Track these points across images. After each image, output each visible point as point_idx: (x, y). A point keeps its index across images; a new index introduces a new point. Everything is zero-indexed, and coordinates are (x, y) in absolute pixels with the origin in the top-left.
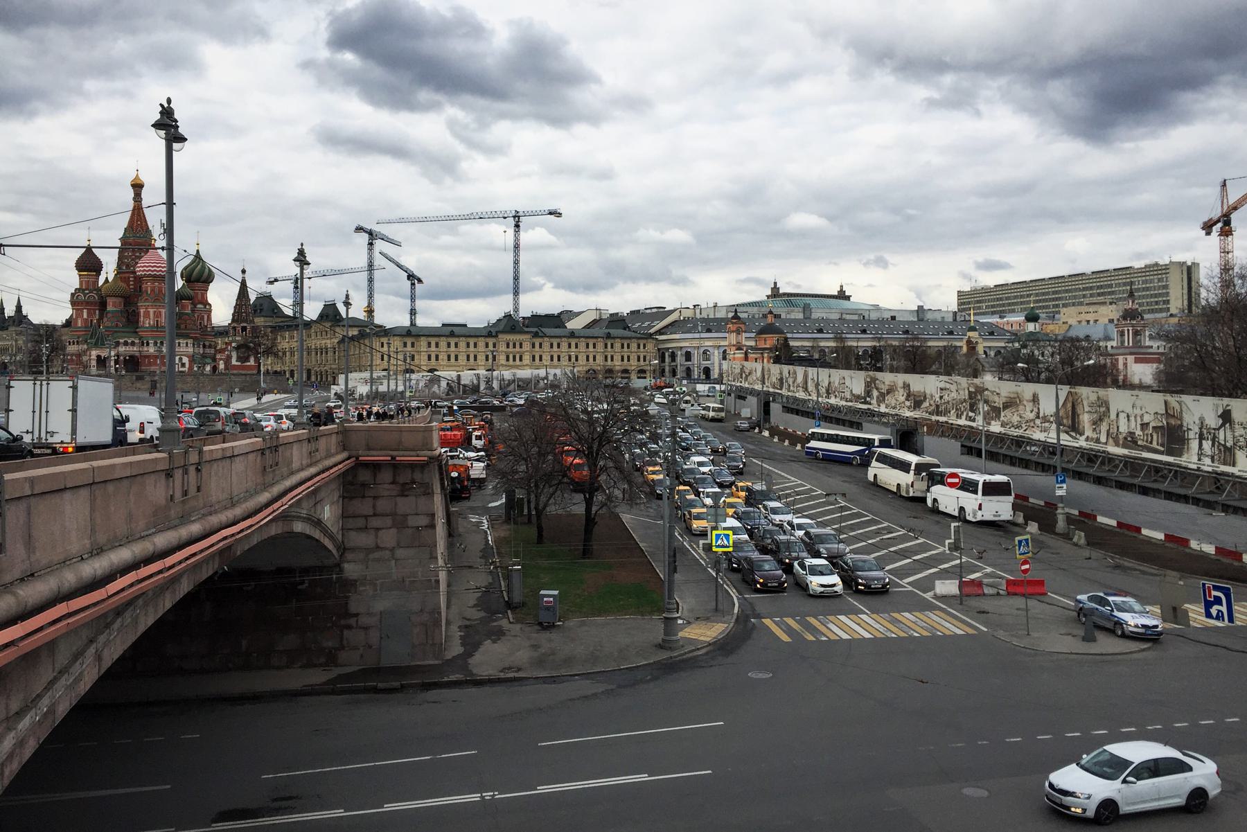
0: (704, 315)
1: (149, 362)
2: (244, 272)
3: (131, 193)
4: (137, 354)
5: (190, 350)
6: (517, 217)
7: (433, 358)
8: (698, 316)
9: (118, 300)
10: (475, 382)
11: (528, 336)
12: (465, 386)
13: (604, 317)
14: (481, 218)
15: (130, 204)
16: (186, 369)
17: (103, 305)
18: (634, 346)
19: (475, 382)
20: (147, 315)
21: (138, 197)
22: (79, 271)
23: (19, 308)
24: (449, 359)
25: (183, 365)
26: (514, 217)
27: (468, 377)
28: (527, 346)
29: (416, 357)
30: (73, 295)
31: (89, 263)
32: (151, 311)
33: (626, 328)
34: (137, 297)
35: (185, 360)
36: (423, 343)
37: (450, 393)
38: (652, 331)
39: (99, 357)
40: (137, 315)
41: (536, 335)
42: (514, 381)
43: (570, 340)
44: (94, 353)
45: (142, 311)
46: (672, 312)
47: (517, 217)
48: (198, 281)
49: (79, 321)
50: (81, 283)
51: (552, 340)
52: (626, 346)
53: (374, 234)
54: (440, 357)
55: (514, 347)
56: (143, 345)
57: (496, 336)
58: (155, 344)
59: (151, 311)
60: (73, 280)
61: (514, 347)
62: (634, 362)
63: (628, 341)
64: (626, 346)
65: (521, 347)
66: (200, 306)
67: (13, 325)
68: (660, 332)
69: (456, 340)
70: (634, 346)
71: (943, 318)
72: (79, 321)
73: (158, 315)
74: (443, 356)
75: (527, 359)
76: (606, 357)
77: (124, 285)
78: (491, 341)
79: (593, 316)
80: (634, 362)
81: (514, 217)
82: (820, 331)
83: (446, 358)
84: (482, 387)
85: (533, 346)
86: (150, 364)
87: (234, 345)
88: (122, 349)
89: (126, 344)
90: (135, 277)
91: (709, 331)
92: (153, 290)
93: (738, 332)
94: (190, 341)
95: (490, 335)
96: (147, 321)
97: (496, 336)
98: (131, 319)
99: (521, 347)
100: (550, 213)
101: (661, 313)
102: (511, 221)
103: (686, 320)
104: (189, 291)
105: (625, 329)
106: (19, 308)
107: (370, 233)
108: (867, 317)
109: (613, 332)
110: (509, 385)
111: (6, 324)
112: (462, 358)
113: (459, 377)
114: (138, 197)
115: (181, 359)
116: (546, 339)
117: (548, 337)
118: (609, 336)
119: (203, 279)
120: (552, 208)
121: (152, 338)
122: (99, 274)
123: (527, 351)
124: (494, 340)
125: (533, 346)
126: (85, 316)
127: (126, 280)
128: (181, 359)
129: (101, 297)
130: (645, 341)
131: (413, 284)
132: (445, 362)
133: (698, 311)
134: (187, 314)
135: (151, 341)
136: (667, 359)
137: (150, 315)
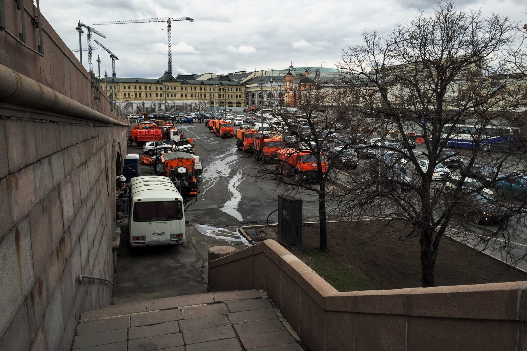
0: (267, 75)
6: (169, 21)
7: (127, 95)
8: (264, 75)
10: (153, 106)
11: (179, 84)
12: (147, 108)
13: (214, 77)
14: (149, 22)
18: (234, 89)
19: (153, 106)
26: (168, 21)
27: (148, 104)
28: (178, 89)
29: (117, 94)
33: (230, 80)
36: (121, 86)
37: (139, 112)
41: (183, 83)
42: (174, 106)
43: (201, 86)
47: (169, 21)
51: (192, 86)
52: (230, 89)
53: (91, 30)
54: (131, 94)
55: (172, 89)
57: (162, 83)
61: (172, 89)
62: (234, 98)
63: (232, 87)
64: (230, 89)
65: (175, 89)
69: (140, 85)
70: (234, 89)
74: (132, 94)
75: (179, 96)
76: (220, 95)
78: (159, 86)
79: (209, 77)
80: (234, 98)
81: (168, 21)
83: (134, 95)
84: (157, 109)
85: (182, 89)
97: (162, 83)
99: (175, 89)
100: (187, 19)
101: (244, 74)
102: (166, 24)
103: (258, 78)
105: (229, 81)
109: (224, 82)
110: (171, 108)
113: (143, 103)
116: (189, 85)
117: (189, 84)
118: (221, 84)
120: (188, 16)
123: (178, 92)
125: (182, 89)
130: (240, 87)
131: (113, 60)
132: (134, 97)
133: (264, 73)
136: (250, 98)
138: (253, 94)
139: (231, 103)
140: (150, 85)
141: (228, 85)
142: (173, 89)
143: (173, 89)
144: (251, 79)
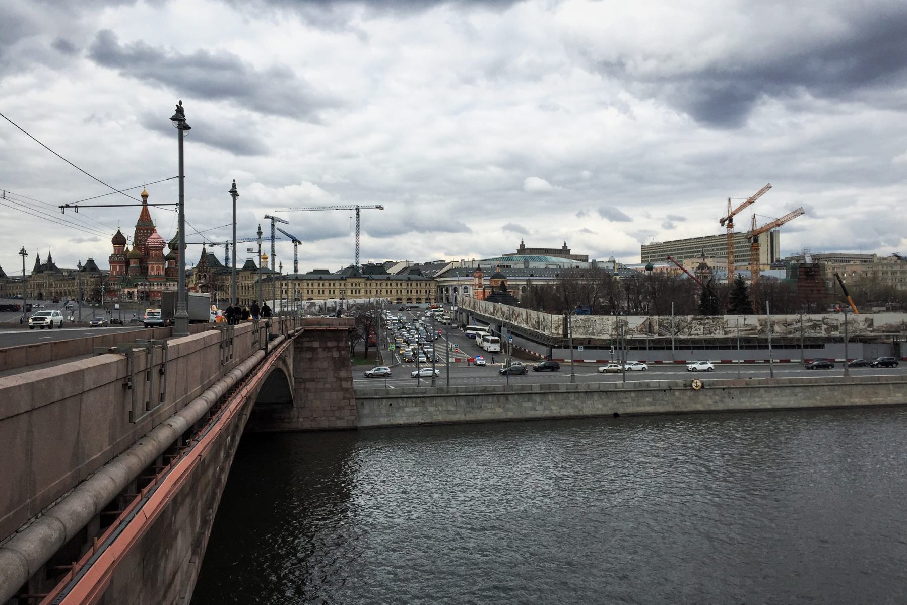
1: (154, 295)
6: (358, 209)
7: (310, 292)
8: (463, 267)
9: (136, 260)
10: (334, 305)
12: (328, 308)
13: (410, 266)
17: (127, 263)
18: (423, 284)
19: (334, 305)
20: (153, 269)
23: (50, 259)
24: (319, 292)
26: (356, 209)
27: (330, 303)
28: (363, 285)
30: (110, 258)
31: (119, 240)
33: (420, 274)
36: (305, 283)
38: (435, 276)
39: (129, 292)
40: (147, 268)
41: (368, 279)
42: (355, 305)
44: (126, 290)
45: (150, 266)
46: (449, 264)
47: (358, 209)
49: (115, 272)
50: (115, 251)
52: (419, 284)
54: (314, 292)
55: (356, 286)
56: (151, 285)
57: (346, 280)
58: (157, 285)
59: (155, 267)
60: (110, 249)
61: (356, 286)
63: (420, 282)
64: (419, 284)
65: (359, 286)
67: (47, 270)
68: (440, 276)
69: (323, 282)
70: (423, 284)
71: (607, 267)
72: (115, 272)
73: (158, 269)
74: (316, 291)
76: (408, 291)
77: (138, 252)
78: (343, 282)
79: (404, 265)
81: (356, 209)
82: (532, 275)
83: (317, 292)
87: (199, 285)
88: (139, 287)
89: (141, 285)
90: (144, 248)
91: (467, 276)
92: (156, 255)
93: (480, 277)
94: (176, 283)
95: (342, 279)
96: (152, 273)
97: (346, 280)
98: (143, 271)
99: (359, 286)
100: (377, 207)
101: (443, 264)
102: (354, 212)
103: (456, 269)
104: (174, 255)
105: (419, 275)
106: (50, 259)
107: (272, 218)
108: (562, 267)
109: (412, 277)
110: (352, 307)
112: (327, 293)
113: (325, 303)
116: (373, 281)
118: (409, 279)
120: (378, 204)
121: (156, 281)
122: (124, 246)
124: (344, 282)
126: (118, 269)
127: (140, 249)
129: (126, 258)
130: (430, 282)
131: (296, 245)
133: (463, 263)
134: (173, 268)
136: (445, 292)
137: (154, 269)
138: (447, 288)
139: (420, 299)
140: (334, 282)
141: (416, 280)
142: (358, 284)
143: (358, 284)
144: (447, 271)
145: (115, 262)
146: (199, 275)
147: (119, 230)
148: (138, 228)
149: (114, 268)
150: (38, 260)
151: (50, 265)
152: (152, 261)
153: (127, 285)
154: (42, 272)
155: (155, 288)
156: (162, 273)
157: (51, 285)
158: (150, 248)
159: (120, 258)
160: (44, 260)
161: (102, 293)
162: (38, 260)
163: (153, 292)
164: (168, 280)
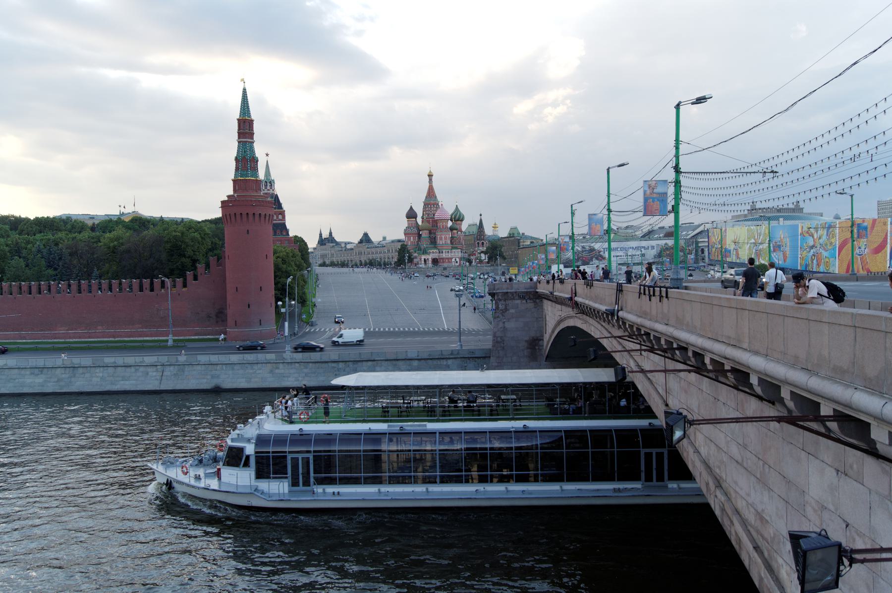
2: (481, 215)
3: (428, 178)
4: (438, 257)
5: (460, 255)
15: (428, 185)
16: (458, 264)
20: (441, 238)
21: (430, 180)
22: (407, 218)
23: (331, 234)
25: (457, 262)
30: (405, 230)
31: (411, 214)
32: (443, 237)
34: (436, 230)
35: (458, 260)
39: (425, 259)
44: (423, 257)
46: (699, 226)
48: (458, 220)
50: (409, 224)
60: (404, 223)
66: (459, 233)
77: (428, 224)
86: (443, 262)
89: (433, 252)
92: (443, 227)
98: (433, 242)
106: (331, 234)
111: (324, 242)
114: (430, 180)
115: (456, 260)
119: (461, 219)
127: (428, 222)
128: (456, 260)
135: (444, 251)
137: (444, 238)
145: (410, 234)
146: (478, 243)
147: (411, 208)
148: (426, 205)
149: (409, 239)
150: (321, 235)
151: (331, 239)
152: (441, 231)
153: (423, 253)
154: (325, 244)
155: (444, 255)
156: (449, 242)
157: (332, 255)
158: (438, 220)
159: (414, 231)
160: (325, 235)
161: (406, 261)
162: (321, 235)
163: (443, 259)
164: (453, 248)
